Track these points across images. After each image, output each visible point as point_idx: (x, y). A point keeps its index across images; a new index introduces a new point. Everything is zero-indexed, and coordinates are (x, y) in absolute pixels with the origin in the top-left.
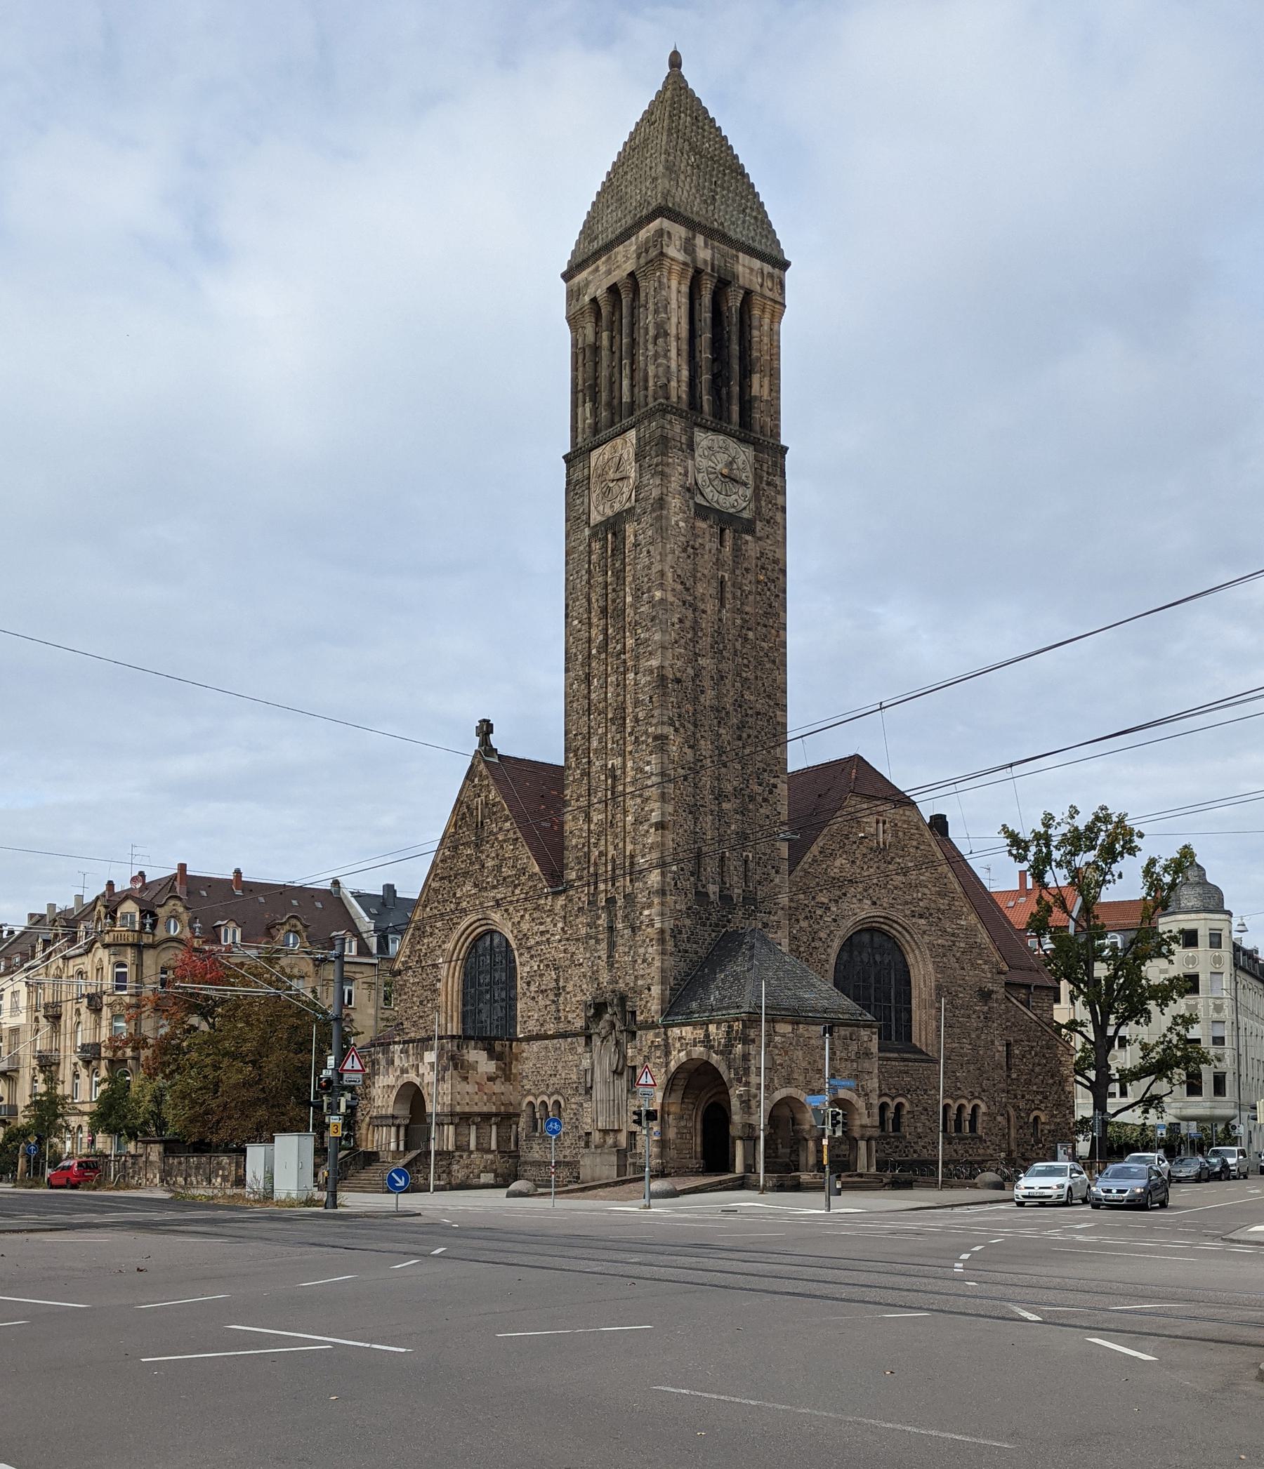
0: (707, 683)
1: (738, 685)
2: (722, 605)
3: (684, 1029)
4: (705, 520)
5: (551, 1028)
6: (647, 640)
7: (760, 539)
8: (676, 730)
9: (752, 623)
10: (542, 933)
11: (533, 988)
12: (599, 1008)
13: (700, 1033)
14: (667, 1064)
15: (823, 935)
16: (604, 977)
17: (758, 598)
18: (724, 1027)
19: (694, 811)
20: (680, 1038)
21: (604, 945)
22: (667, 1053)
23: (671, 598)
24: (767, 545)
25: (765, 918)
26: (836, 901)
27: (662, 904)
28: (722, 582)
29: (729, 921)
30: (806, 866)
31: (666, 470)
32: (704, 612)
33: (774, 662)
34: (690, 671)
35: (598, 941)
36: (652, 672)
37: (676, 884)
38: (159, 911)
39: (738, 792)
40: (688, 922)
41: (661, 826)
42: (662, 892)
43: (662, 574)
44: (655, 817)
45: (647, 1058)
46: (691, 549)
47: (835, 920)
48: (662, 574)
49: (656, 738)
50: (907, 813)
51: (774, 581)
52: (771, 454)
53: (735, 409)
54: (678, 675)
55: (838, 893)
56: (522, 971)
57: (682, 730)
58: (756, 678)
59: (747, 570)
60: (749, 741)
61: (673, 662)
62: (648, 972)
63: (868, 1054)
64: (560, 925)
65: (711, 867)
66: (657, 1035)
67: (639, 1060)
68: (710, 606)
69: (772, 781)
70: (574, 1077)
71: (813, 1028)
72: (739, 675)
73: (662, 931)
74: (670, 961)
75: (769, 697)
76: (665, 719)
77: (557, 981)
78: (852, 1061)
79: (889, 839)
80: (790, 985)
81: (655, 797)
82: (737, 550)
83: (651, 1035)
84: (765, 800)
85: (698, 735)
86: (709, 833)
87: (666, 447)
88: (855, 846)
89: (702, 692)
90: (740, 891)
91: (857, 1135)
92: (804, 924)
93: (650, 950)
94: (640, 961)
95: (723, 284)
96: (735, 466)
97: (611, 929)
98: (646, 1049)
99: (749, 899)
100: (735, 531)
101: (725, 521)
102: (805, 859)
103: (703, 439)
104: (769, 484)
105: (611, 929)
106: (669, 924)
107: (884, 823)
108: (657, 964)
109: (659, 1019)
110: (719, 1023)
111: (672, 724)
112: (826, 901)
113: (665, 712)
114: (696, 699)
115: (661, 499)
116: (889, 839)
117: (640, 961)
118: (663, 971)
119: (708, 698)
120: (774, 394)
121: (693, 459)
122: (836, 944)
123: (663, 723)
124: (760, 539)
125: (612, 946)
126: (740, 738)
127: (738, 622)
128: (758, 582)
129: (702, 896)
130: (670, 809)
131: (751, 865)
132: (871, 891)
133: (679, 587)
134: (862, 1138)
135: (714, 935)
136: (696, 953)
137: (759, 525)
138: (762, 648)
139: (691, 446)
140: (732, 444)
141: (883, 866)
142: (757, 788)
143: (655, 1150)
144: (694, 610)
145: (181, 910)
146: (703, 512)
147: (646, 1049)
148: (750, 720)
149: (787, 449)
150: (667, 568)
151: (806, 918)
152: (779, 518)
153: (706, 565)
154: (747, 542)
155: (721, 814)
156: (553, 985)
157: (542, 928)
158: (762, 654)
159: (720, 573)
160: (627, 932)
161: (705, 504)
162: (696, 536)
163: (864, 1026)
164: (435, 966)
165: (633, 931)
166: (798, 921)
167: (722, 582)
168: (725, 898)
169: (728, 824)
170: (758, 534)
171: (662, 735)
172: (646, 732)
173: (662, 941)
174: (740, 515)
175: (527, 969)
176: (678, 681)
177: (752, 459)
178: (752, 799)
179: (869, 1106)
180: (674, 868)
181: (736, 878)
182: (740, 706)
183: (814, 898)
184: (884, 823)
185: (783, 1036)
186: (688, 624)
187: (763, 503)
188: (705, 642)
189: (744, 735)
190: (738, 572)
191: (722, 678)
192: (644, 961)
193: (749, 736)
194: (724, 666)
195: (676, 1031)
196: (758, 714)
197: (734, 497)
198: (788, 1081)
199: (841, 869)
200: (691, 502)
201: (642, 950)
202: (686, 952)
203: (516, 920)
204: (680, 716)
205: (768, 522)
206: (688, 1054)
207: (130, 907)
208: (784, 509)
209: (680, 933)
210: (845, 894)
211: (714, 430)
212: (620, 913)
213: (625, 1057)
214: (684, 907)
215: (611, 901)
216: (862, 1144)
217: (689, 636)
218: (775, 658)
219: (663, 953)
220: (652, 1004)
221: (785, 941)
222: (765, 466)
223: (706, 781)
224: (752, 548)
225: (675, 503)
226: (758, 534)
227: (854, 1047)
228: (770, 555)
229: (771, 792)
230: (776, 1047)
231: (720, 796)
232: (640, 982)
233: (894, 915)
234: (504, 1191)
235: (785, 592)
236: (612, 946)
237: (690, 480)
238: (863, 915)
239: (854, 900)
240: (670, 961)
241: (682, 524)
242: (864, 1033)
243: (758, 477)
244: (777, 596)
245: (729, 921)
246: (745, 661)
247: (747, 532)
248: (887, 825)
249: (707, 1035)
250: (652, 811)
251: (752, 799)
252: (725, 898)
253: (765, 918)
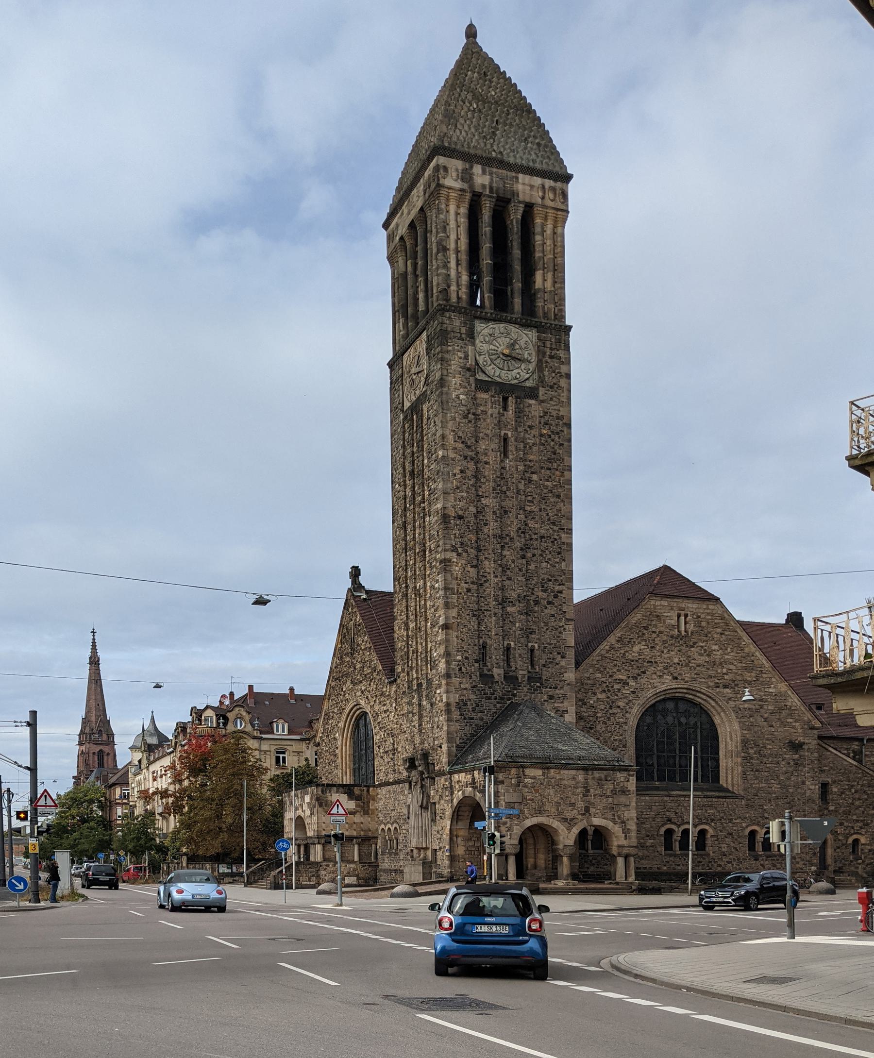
0: (490, 517)
1: (522, 517)
2: (505, 454)
3: (461, 775)
4: (487, 391)
7: (543, 401)
8: (459, 555)
9: (536, 467)
10: (385, 711)
11: (382, 751)
15: (621, 704)
16: (417, 740)
17: (542, 447)
19: (479, 614)
20: (459, 782)
21: (416, 717)
23: (452, 455)
24: (551, 406)
25: (551, 692)
26: (635, 678)
27: (447, 684)
29: (514, 695)
30: (603, 652)
31: (446, 356)
32: (486, 463)
33: (559, 496)
34: (473, 509)
37: (460, 669)
38: (228, 715)
39: (520, 599)
40: (473, 697)
42: (448, 676)
43: (443, 437)
44: (442, 621)
45: (441, 796)
46: (473, 416)
47: (633, 692)
48: (443, 437)
50: (711, 607)
51: (558, 433)
52: (555, 333)
53: (517, 302)
54: (460, 513)
55: (637, 671)
56: (377, 738)
57: (465, 554)
58: (540, 510)
59: (530, 427)
60: (534, 559)
61: (456, 504)
62: (439, 735)
63: (624, 791)
64: (394, 705)
65: (495, 656)
68: (493, 458)
69: (557, 588)
71: (566, 772)
72: (522, 508)
73: (448, 704)
74: (456, 726)
75: (554, 524)
76: (448, 547)
77: (393, 744)
78: (608, 797)
79: (691, 627)
80: (549, 740)
81: (441, 606)
82: (519, 412)
84: (549, 603)
85: (482, 558)
86: (493, 630)
87: (446, 338)
88: (654, 635)
89: (486, 524)
90: (525, 673)
91: (615, 853)
92: (602, 696)
93: (441, 719)
96: (517, 347)
97: (420, 705)
98: (440, 790)
100: (517, 398)
101: (506, 392)
102: (602, 647)
104: (551, 357)
106: (455, 698)
107: (686, 616)
108: (445, 728)
109: (446, 768)
112: (624, 678)
113: (448, 542)
114: (478, 530)
115: (442, 379)
116: (691, 627)
118: (448, 733)
119: (492, 527)
120: (558, 285)
121: (474, 344)
122: (635, 712)
123: (445, 550)
124: (543, 401)
125: (421, 717)
126: (523, 557)
127: (521, 468)
128: (541, 435)
129: (487, 678)
130: (454, 613)
131: (537, 653)
132: (672, 669)
133: (460, 446)
134: (620, 855)
135: (498, 706)
136: (482, 719)
137: (542, 391)
138: (546, 487)
140: (513, 329)
141: (684, 648)
142: (541, 594)
143: (447, 862)
144: (476, 463)
145: (244, 714)
146: (483, 386)
147: (440, 790)
148: (535, 543)
149: (571, 327)
150: (447, 432)
151: (604, 691)
152: (563, 383)
153: (487, 426)
154: (530, 405)
155: (505, 616)
156: (391, 748)
157: (385, 708)
158: (545, 491)
159: (503, 433)
160: (428, 706)
161: (487, 379)
162: (477, 405)
163: (620, 770)
164: (335, 739)
166: (595, 694)
168: (511, 679)
169: (514, 624)
170: (541, 398)
171: (445, 559)
173: (448, 711)
174: (523, 384)
175: (378, 737)
176: (460, 517)
177: (535, 339)
178: (537, 603)
180: (459, 658)
181: (520, 663)
182: (523, 533)
183: (611, 676)
184: (686, 616)
185: (534, 778)
186: (469, 473)
187: (546, 373)
188: (487, 487)
189: (529, 555)
190: (519, 429)
191: (506, 512)
192: (438, 727)
193: (534, 555)
194: (508, 503)
195: (456, 776)
196: (542, 537)
197: (516, 371)
198: (540, 812)
199: (640, 653)
200: (472, 379)
201: (436, 719)
202: (472, 719)
204: (462, 544)
205: (551, 387)
206: (463, 793)
207: (209, 713)
208: (568, 376)
209: (466, 705)
210: (644, 673)
211: (494, 320)
213: (429, 796)
214: (468, 686)
215: (420, 685)
217: (471, 482)
218: (562, 492)
219: (449, 720)
220: (442, 759)
222: (548, 344)
223: (490, 590)
224: (534, 408)
226: (541, 398)
227: (609, 786)
228: (554, 414)
229: (556, 596)
230: (525, 786)
231: (503, 602)
232: (436, 742)
233: (696, 686)
234: (315, 890)
235: (570, 440)
236: (421, 717)
238: (664, 687)
239: (654, 676)
240: (456, 726)
241: (462, 397)
242: (621, 776)
243: (540, 352)
244: (562, 445)
245: (514, 695)
246: (529, 498)
247: (531, 398)
248: (689, 618)
250: (440, 616)
251: (537, 603)
252: (511, 679)
253: (551, 692)
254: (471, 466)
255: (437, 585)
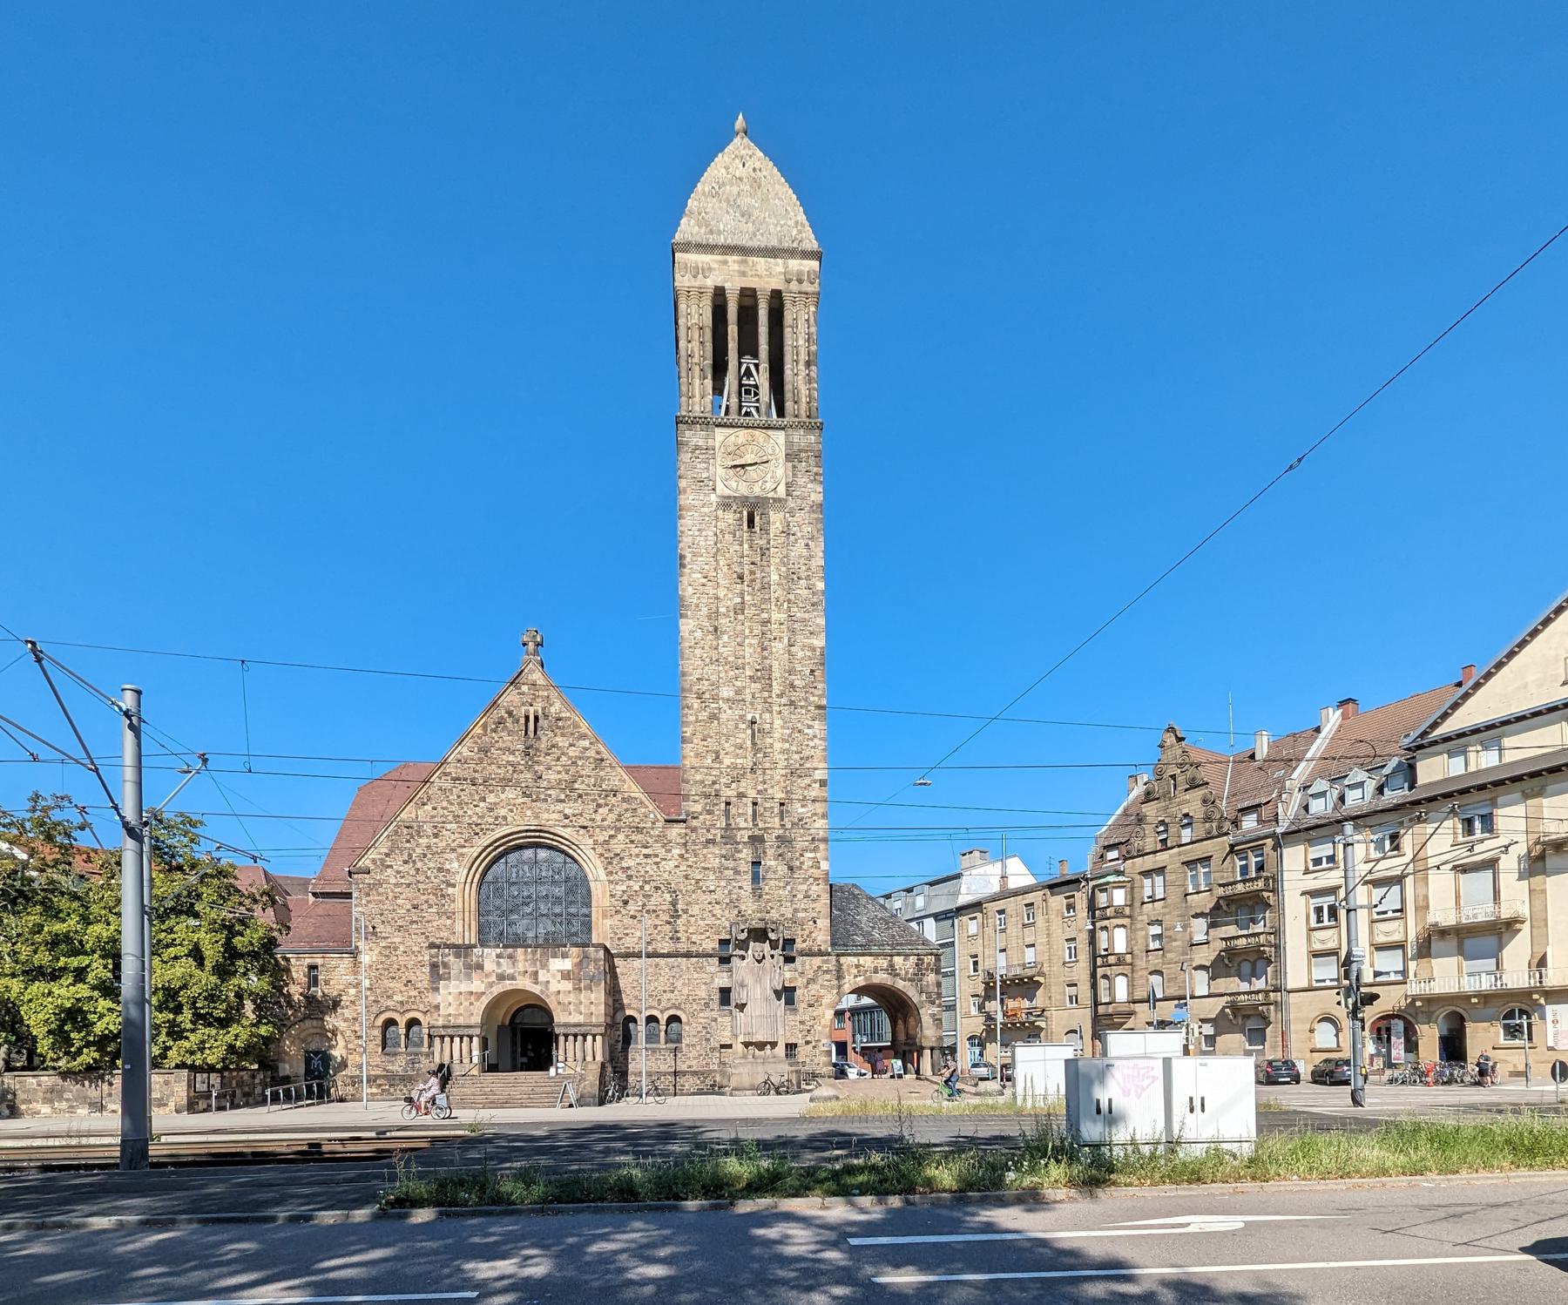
5: (666, 947)
6: (804, 620)
13: (883, 963)
14: (839, 987)
18: (913, 959)
22: (839, 977)
35: (737, 872)
36: (814, 650)
66: (826, 962)
67: (800, 982)
70: (704, 995)
83: (817, 961)
94: (800, 896)
105: (756, 864)
110: (907, 956)
117: (800, 896)
160: (782, 869)
165: (791, 869)
172: (806, 700)
203: (601, 839)
212: (770, 852)
232: (800, 915)
249: (892, 966)
255: (809, 731)
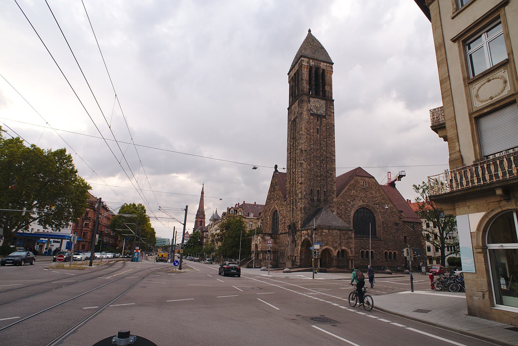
12: (289, 227)
23: (304, 133)
28: (318, 129)
41: (301, 183)
49: (301, 163)
74: (303, 215)
95: (317, 69)
99: (326, 200)
101: (319, 117)
103: (312, 100)
106: (303, 206)
111: (304, 160)
122: (353, 212)
129: (312, 200)
130: (303, 179)
139: (309, 101)
146: (312, 115)
167: (318, 129)
176: (306, 151)
179: (351, 251)
215: (293, 202)
216: (350, 261)
219: (301, 213)
221: (336, 211)
225: (305, 113)
237: (309, 108)
240: (303, 215)
254: (309, 136)
